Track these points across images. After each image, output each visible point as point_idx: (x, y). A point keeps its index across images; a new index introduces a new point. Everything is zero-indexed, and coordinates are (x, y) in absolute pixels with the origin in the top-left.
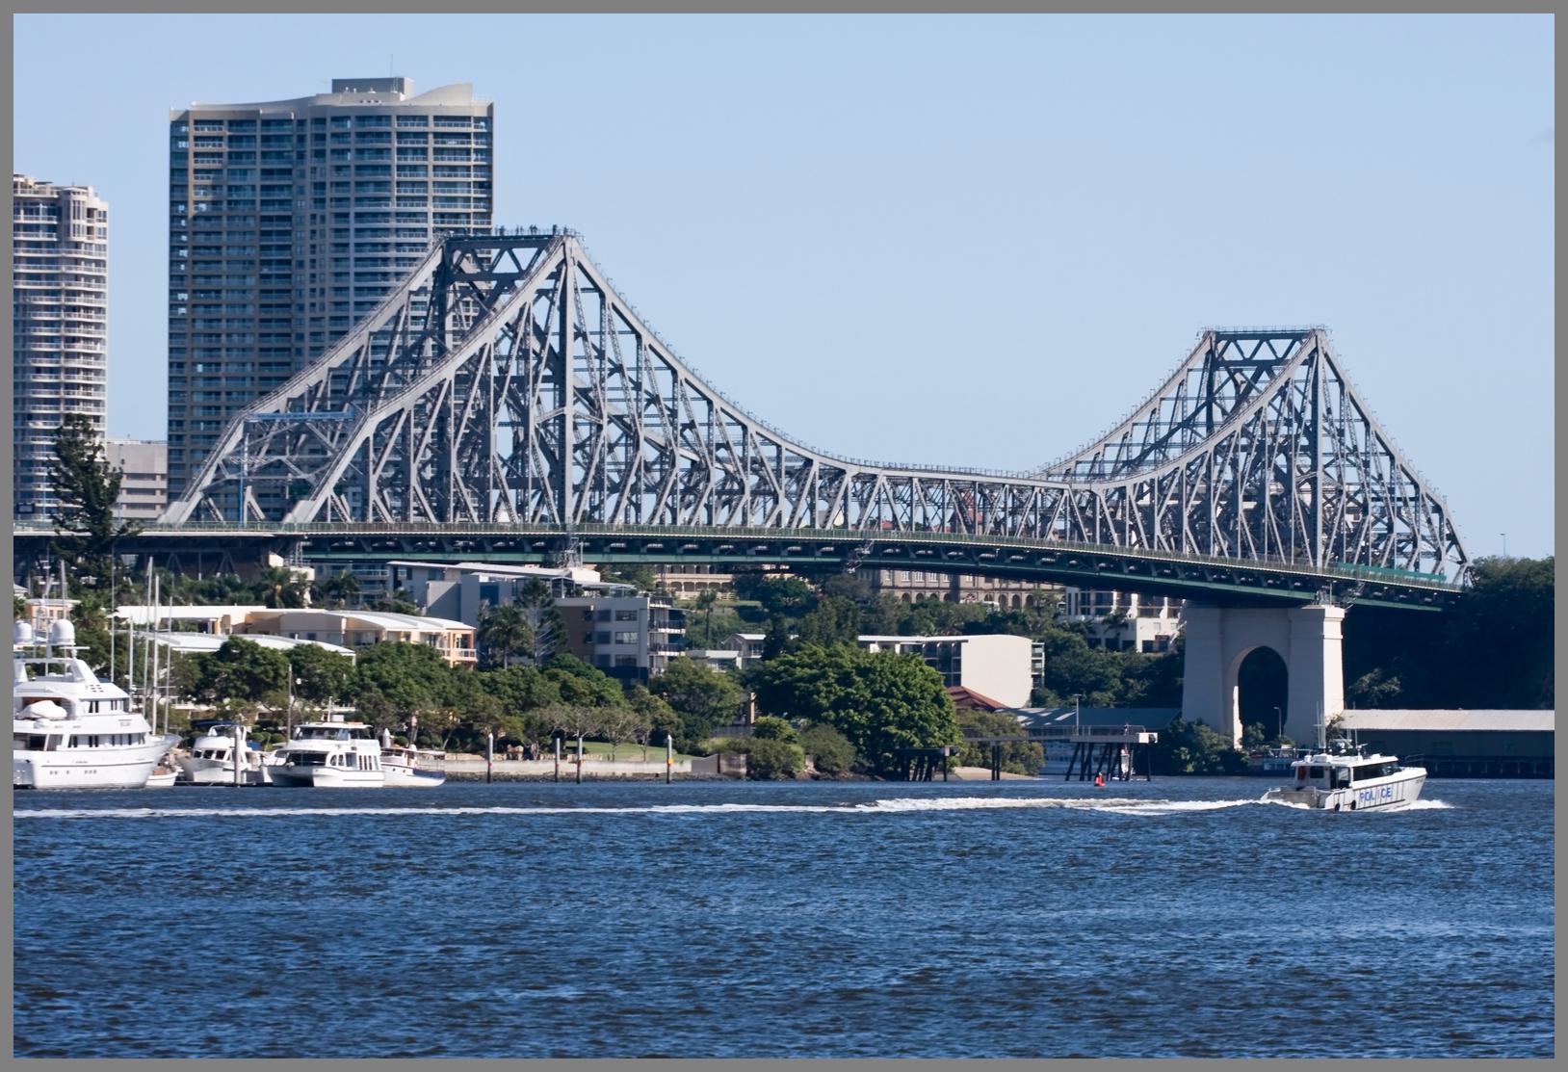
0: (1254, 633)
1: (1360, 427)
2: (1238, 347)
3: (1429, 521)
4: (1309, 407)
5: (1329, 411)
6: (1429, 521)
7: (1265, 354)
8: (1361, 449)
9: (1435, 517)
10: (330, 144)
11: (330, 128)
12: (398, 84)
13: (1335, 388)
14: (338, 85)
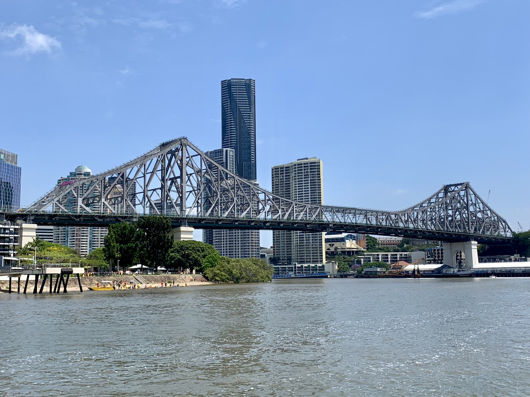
0: (457, 246)
1: (481, 205)
2: (451, 188)
3: (502, 224)
4: (466, 198)
5: (472, 200)
6: (502, 224)
7: (456, 189)
8: (482, 209)
9: (504, 224)
10: (293, 170)
11: (293, 167)
12: (307, 159)
13: (473, 196)
14: (298, 160)
